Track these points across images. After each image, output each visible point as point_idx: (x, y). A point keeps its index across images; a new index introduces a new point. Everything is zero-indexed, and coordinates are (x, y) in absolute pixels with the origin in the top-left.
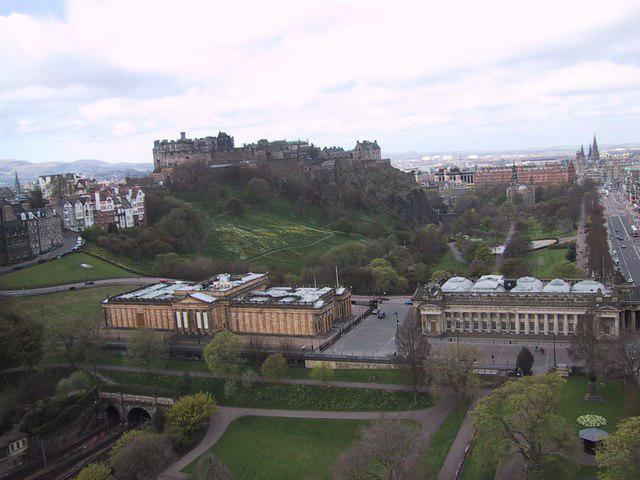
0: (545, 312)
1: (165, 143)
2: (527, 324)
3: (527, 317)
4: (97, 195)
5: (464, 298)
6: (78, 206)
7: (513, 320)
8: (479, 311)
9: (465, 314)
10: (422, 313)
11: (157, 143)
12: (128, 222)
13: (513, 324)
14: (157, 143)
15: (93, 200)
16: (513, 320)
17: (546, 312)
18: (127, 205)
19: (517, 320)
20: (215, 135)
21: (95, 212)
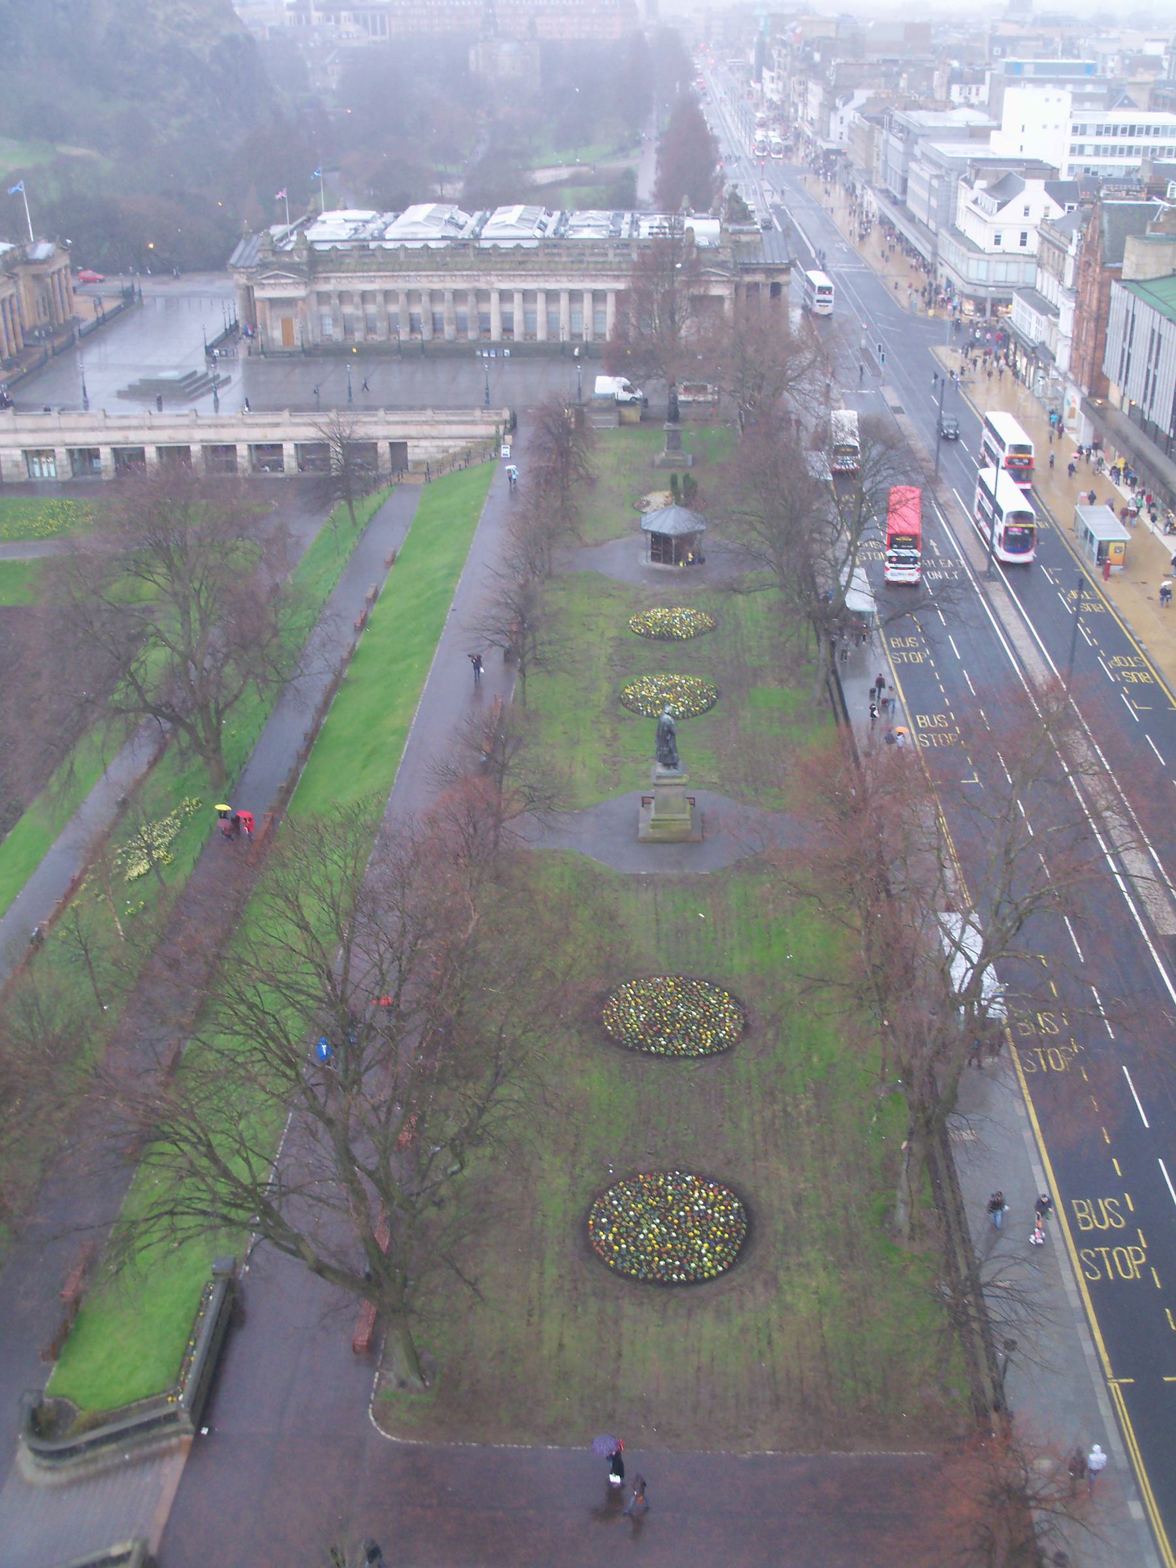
0: (562, 284)
2: (518, 317)
3: (518, 298)
5: (362, 254)
7: (484, 308)
8: (400, 285)
9: (365, 296)
10: (258, 294)
13: (484, 319)
16: (484, 308)
17: (562, 284)
19: (493, 308)
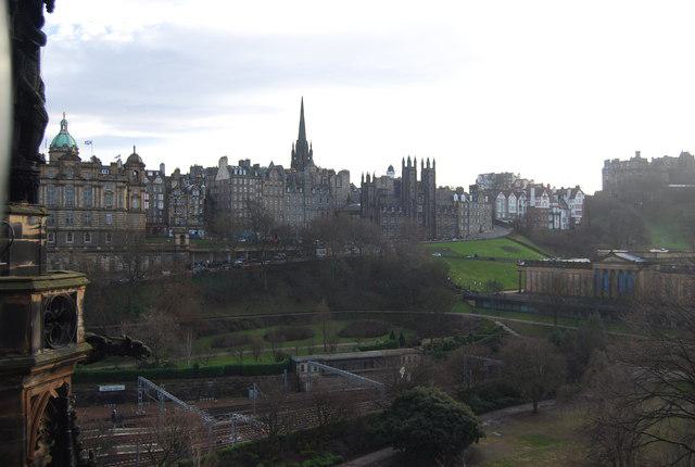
1: (616, 161)
4: (533, 190)
6: (512, 198)
11: (607, 162)
12: (560, 223)
14: (607, 162)
15: (528, 196)
18: (565, 206)
20: (676, 154)
21: (529, 208)
